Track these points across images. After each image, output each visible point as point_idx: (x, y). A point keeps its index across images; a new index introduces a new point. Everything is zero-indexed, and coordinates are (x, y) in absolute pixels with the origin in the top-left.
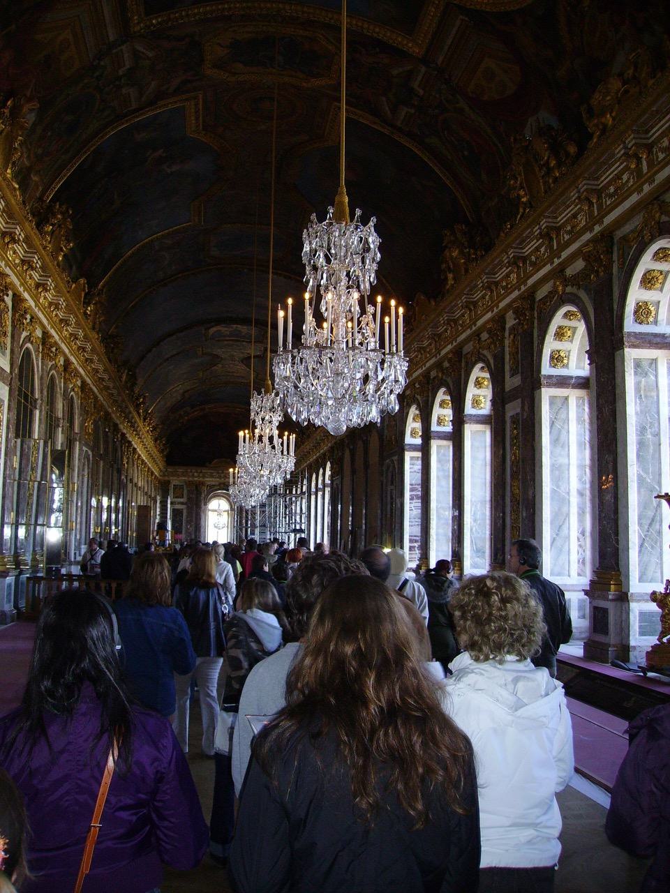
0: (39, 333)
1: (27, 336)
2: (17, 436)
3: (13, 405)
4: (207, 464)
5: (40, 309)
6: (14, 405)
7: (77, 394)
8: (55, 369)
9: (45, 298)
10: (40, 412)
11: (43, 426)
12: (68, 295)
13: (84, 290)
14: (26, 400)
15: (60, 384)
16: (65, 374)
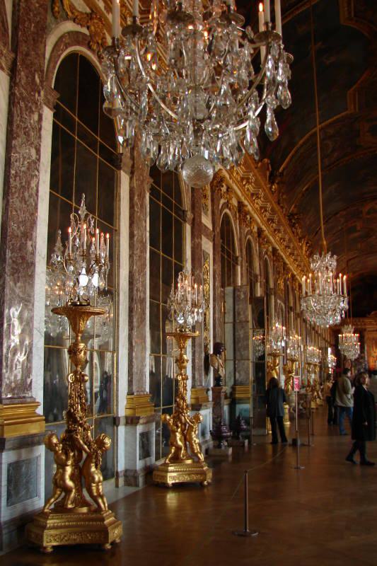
0: (234, 202)
1: (224, 203)
2: (223, 286)
3: (217, 257)
4: (368, 316)
5: (234, 181)
6: (218, 258)
7: (270, 257)
8: (250, 234)
9: (237, 173)
10: (242, 268)
11: (245, 279)
12: (256, 171)
13: (268, 169)
14: (229, 255)
15: (255, 247)
16: (259, 240)
